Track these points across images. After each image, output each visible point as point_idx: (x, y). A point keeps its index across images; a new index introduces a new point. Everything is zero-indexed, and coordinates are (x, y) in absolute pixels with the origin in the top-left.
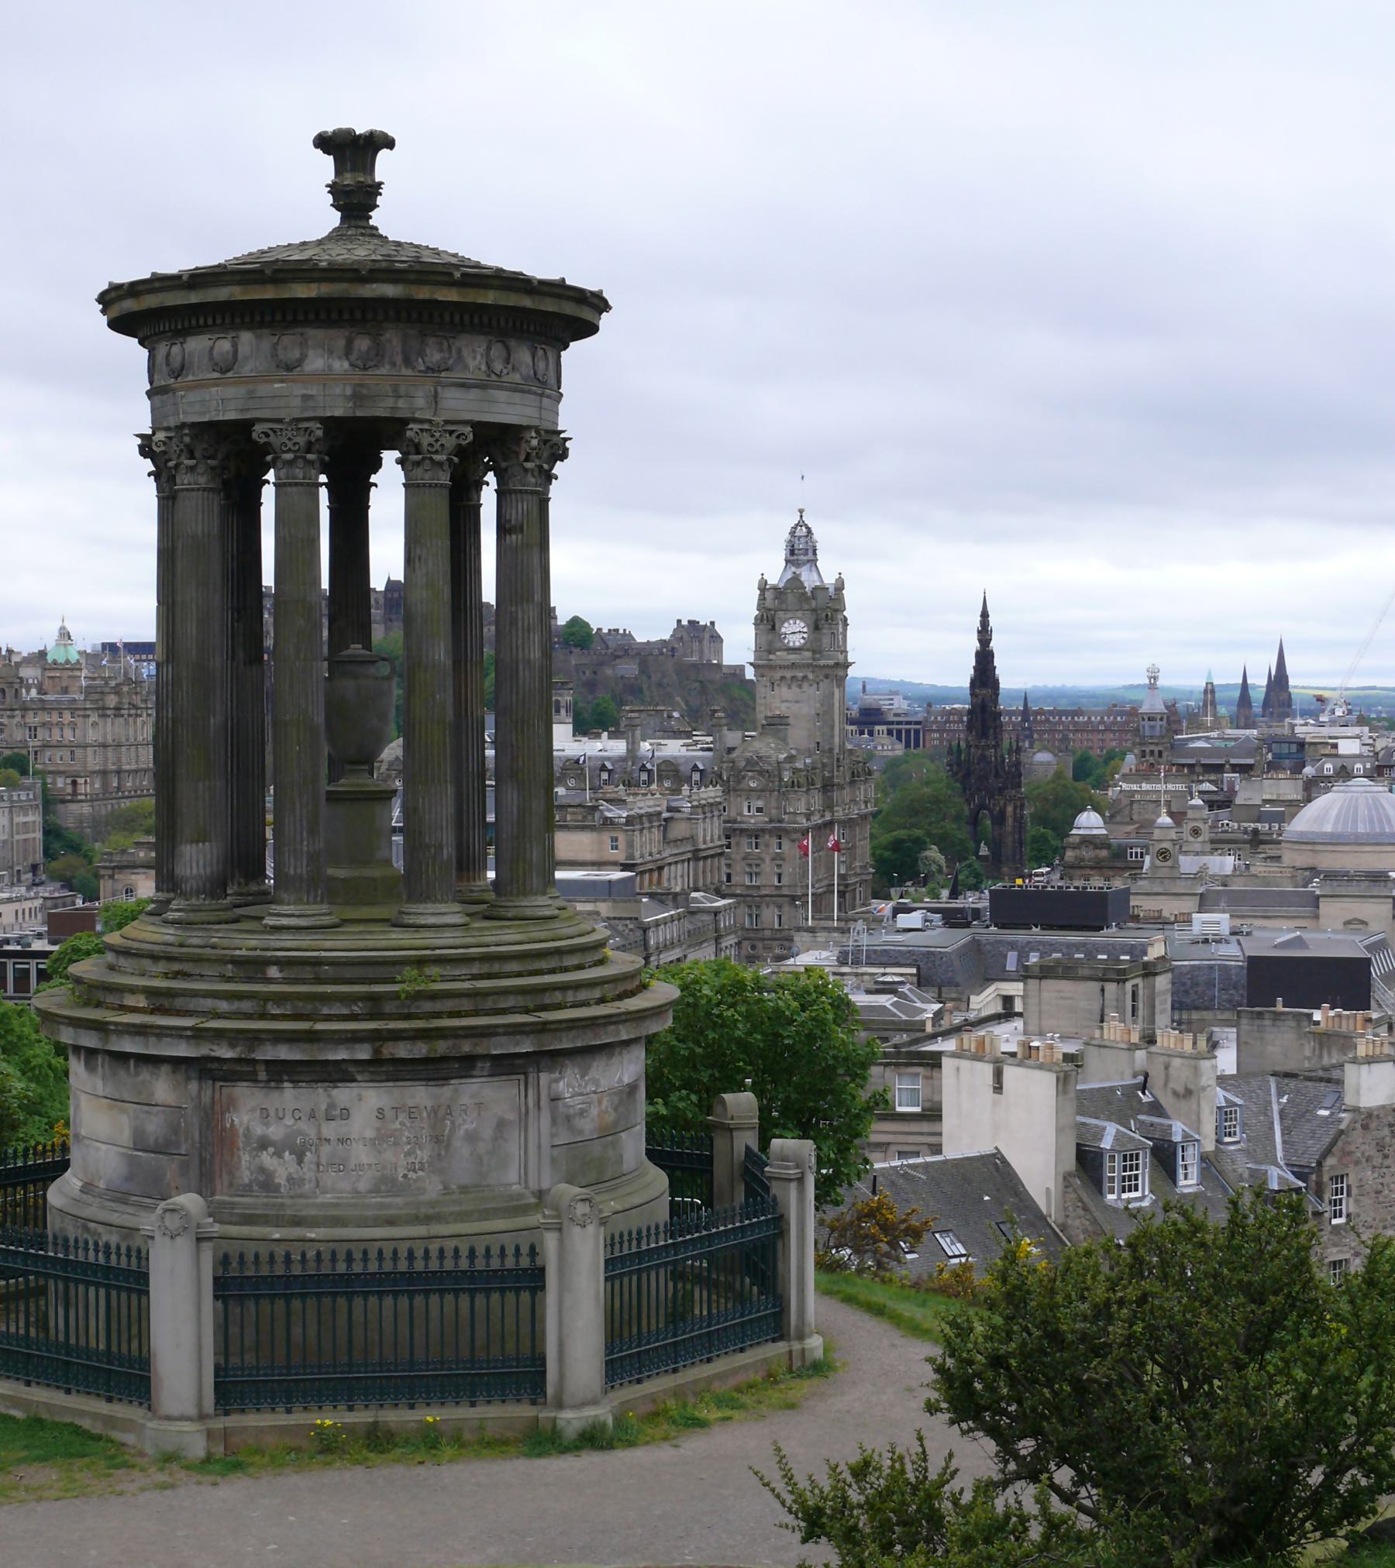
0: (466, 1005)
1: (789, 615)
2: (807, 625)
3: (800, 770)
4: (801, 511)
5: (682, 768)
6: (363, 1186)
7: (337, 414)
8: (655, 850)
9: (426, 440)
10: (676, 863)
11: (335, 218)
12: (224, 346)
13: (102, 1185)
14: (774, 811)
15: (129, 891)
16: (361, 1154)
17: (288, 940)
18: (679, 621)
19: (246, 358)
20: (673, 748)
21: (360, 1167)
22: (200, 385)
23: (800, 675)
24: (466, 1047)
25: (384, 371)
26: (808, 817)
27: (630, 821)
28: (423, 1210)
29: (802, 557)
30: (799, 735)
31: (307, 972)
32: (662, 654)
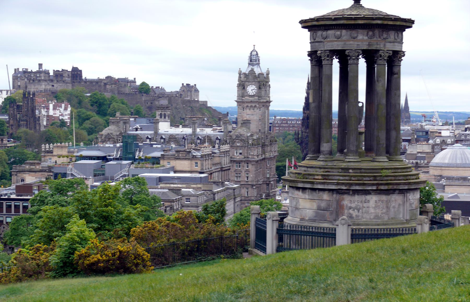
0: (393, 178)
2: (256, 87)
3: (255, 139)
4: (254, 46)
5: (212, 138)
6: (372, 217)
7: (365, 48)
8: (209, 167)
9: (383, 54)
12: (338, 33)
14: (246, 154)
15: (23, 180)
16: (372, 210)
17: (352, 164)
18: (183, 84)
20: (208, 131)
21: (371, 213)
24: (395, 187)
25: (375, 39)
26: (258, 156)
27: (202, 156)
28: (385, 223)
29: (254, 63)
30: (254, 127)
31: (358, 171)
32: (177, 96)
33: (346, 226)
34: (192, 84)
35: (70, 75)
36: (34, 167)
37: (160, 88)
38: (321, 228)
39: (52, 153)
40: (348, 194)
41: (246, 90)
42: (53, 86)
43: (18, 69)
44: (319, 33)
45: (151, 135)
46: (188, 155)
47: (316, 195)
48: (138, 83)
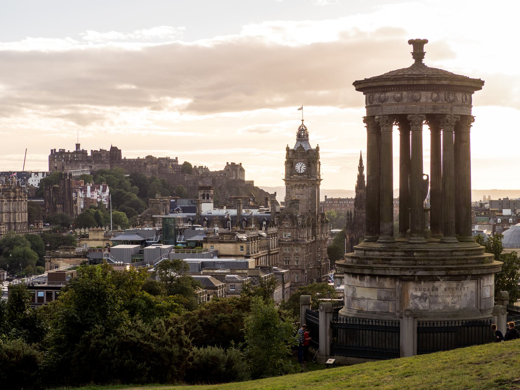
1: (299, 160)
2: (306, 165)
4: (303, 120)
7: (429, 112)
9: (450, 119)
11: (413, 61)
18: (227, 163)
22: (392, 105)
24: (467, 272)
25: (440, 102)
26: (308, 238)
34: (237, 163)
35: (109, 155)
36: (68, 253)
37: (204, 167)
39: (88, 237)
40: (413, 280)
41: (295, 168)
42: (91, 167)
43: (55, 150)
44: (377, 95)
45: (193, 217)
48: (181, 162)
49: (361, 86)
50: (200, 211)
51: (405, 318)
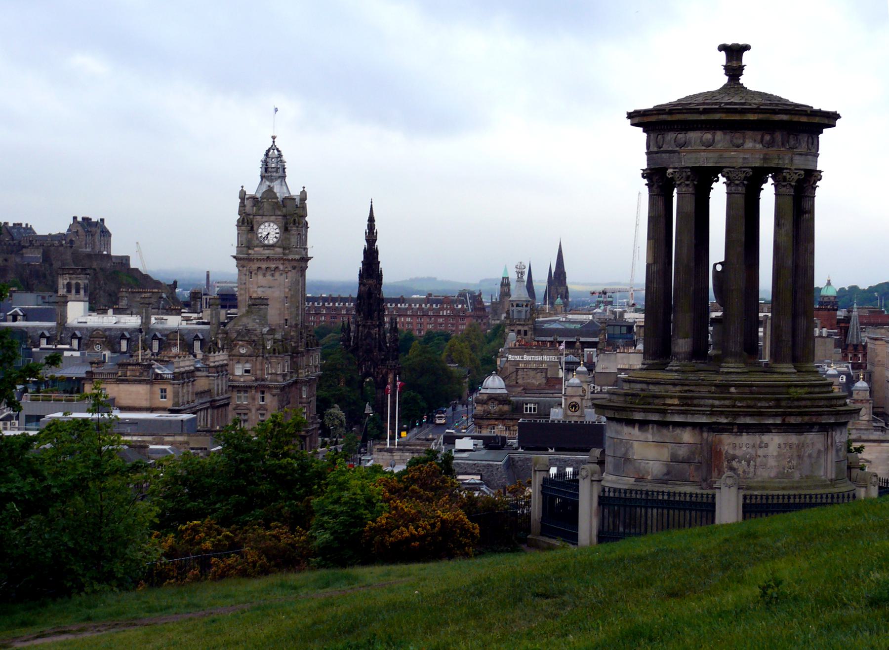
0: (809, 403)
1: (265, 219)
2: (280, 228)
3: (278, 340)
4: (274, 138)
6: (772, 475)
9: (788, 176)
10: (201, 410)
11: (725, 79)
12: (708, 136)
13: (649, 477)
14: (258, 372)
16: (772, 462)
17: (734, 377)
18: (75, 218)
19: (719, 142)
21: (772, 467)
23: (273, 266)
27: (176, 376)
28: (796, 485)
29: (274, 174)
31: (747, 390)
32: (62, 245)
33: (734, 490)
37: (24, 226)
38: (680, 494)
40: (730, 431)
44: (670, 136)
46: (145, 373)
47: (668, 434)
49: (638, 118)
50: (64, 316)
51: (724, 490)
